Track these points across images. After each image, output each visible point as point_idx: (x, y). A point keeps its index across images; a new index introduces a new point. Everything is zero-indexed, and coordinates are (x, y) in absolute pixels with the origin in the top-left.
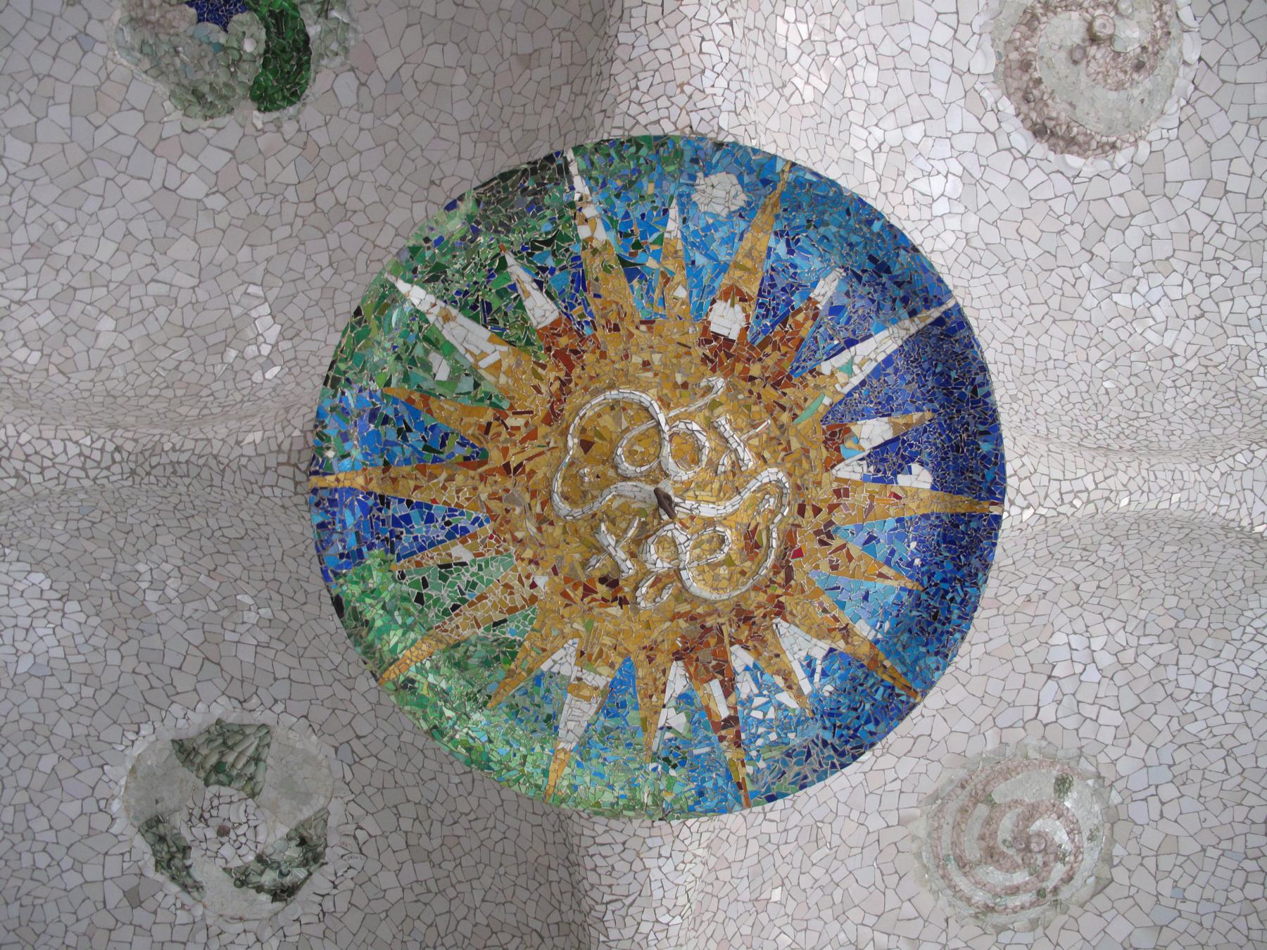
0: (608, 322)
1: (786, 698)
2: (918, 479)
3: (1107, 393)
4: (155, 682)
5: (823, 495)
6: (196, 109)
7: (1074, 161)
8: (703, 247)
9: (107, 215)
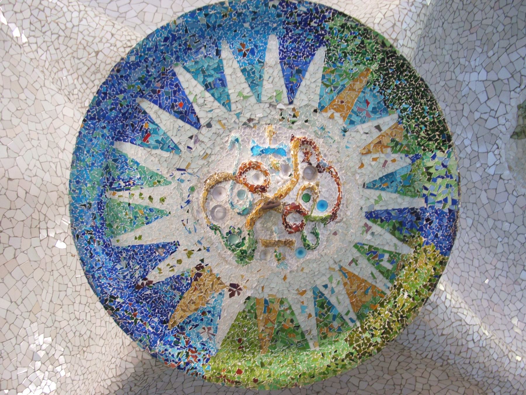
4: (485, 116)
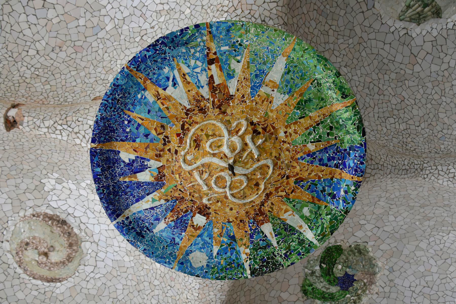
0: (244, 223)
1: (186, 70)
2: (126, 156)
3: (33, 141)
4: (439, 48)
6: (362, 247)
7: (50, 212)
8: (205, 243)
9: (402, 223)
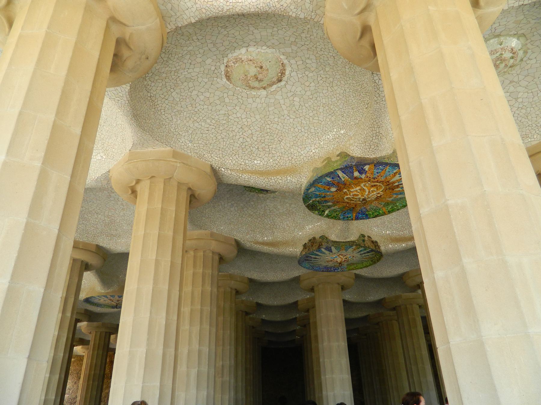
5: (367, 179)
7: (287, 73)
8: (320, 191)
